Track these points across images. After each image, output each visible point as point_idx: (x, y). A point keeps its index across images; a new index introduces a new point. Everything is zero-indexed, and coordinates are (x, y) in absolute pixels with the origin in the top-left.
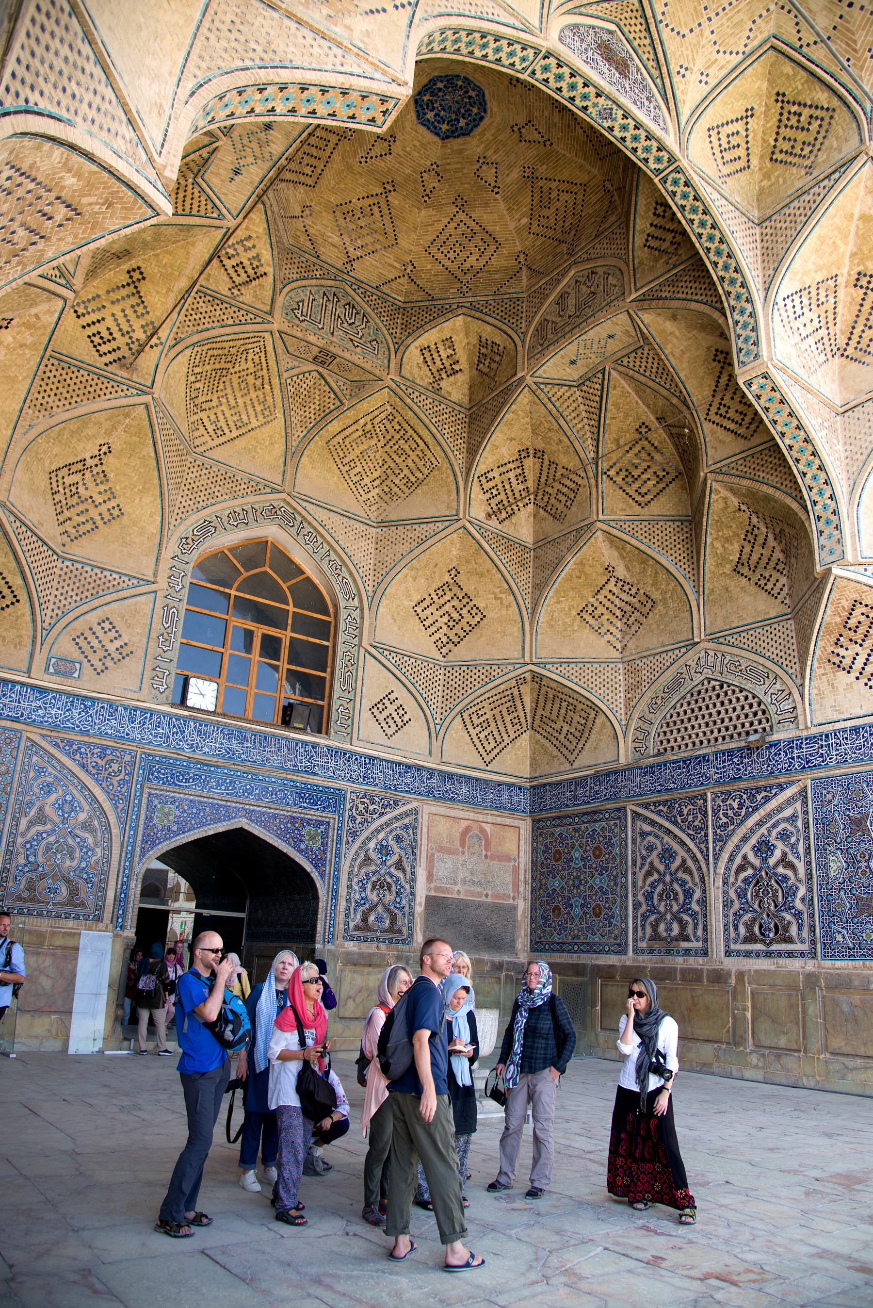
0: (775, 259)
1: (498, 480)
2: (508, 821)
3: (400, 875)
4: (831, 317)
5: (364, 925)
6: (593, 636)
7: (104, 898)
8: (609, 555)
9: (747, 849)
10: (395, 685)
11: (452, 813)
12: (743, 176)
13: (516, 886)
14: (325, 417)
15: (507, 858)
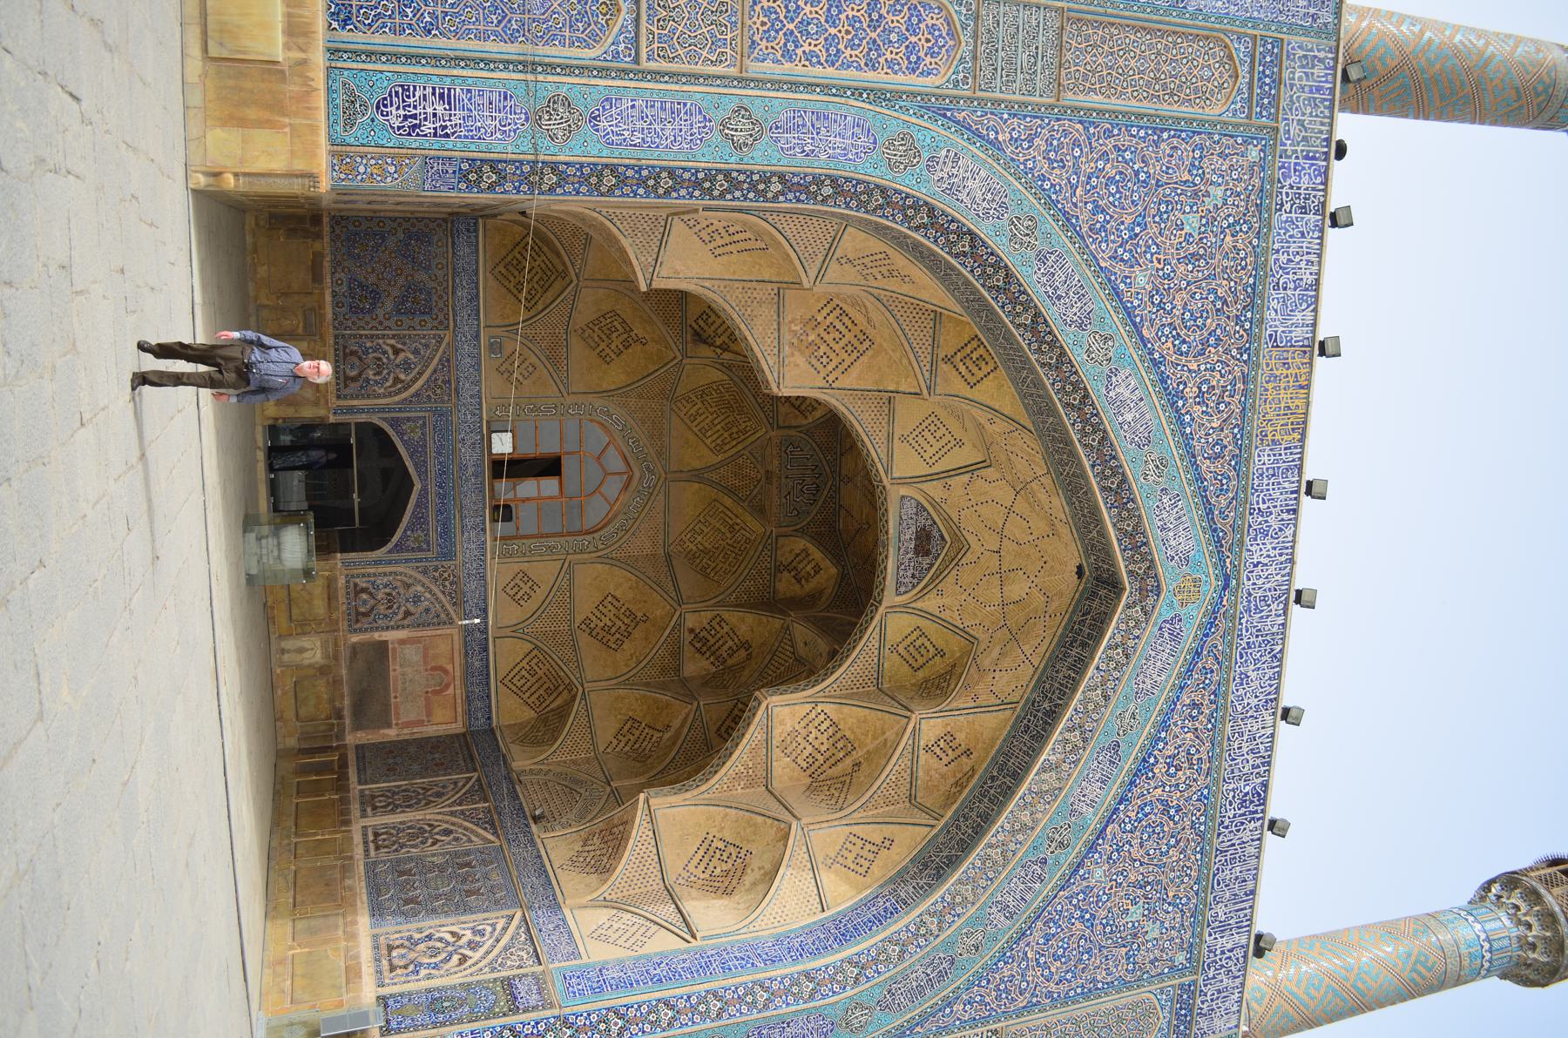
0: (849, 697)
1: (723, 632)
2: (459, 710)
3: (400, 616)
4: (832, 761)
5: (358, 591)
6: (613, 731)
7: (352, 398)
8: (676, 723)
9: (445, 826)
10: (545, 588)
11: (456, 655)
12: (906, 668)
13: (409, 724)
14: (731, 491)
15: (429, 714)
